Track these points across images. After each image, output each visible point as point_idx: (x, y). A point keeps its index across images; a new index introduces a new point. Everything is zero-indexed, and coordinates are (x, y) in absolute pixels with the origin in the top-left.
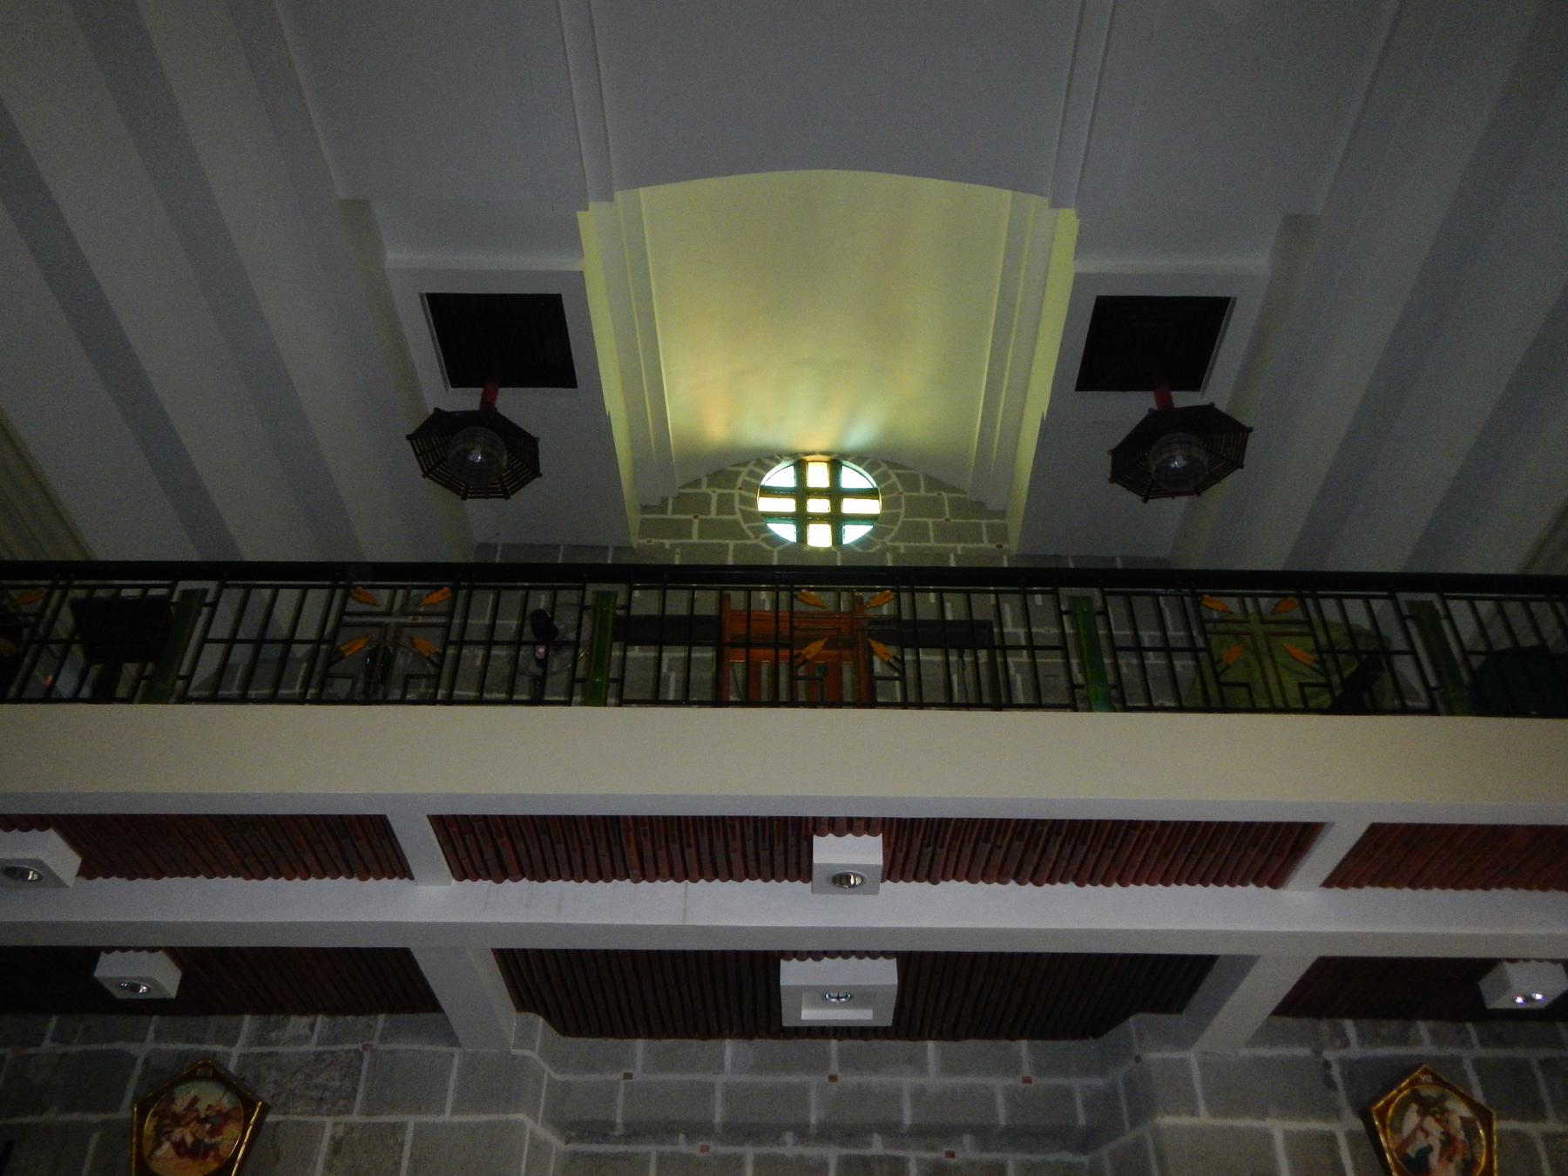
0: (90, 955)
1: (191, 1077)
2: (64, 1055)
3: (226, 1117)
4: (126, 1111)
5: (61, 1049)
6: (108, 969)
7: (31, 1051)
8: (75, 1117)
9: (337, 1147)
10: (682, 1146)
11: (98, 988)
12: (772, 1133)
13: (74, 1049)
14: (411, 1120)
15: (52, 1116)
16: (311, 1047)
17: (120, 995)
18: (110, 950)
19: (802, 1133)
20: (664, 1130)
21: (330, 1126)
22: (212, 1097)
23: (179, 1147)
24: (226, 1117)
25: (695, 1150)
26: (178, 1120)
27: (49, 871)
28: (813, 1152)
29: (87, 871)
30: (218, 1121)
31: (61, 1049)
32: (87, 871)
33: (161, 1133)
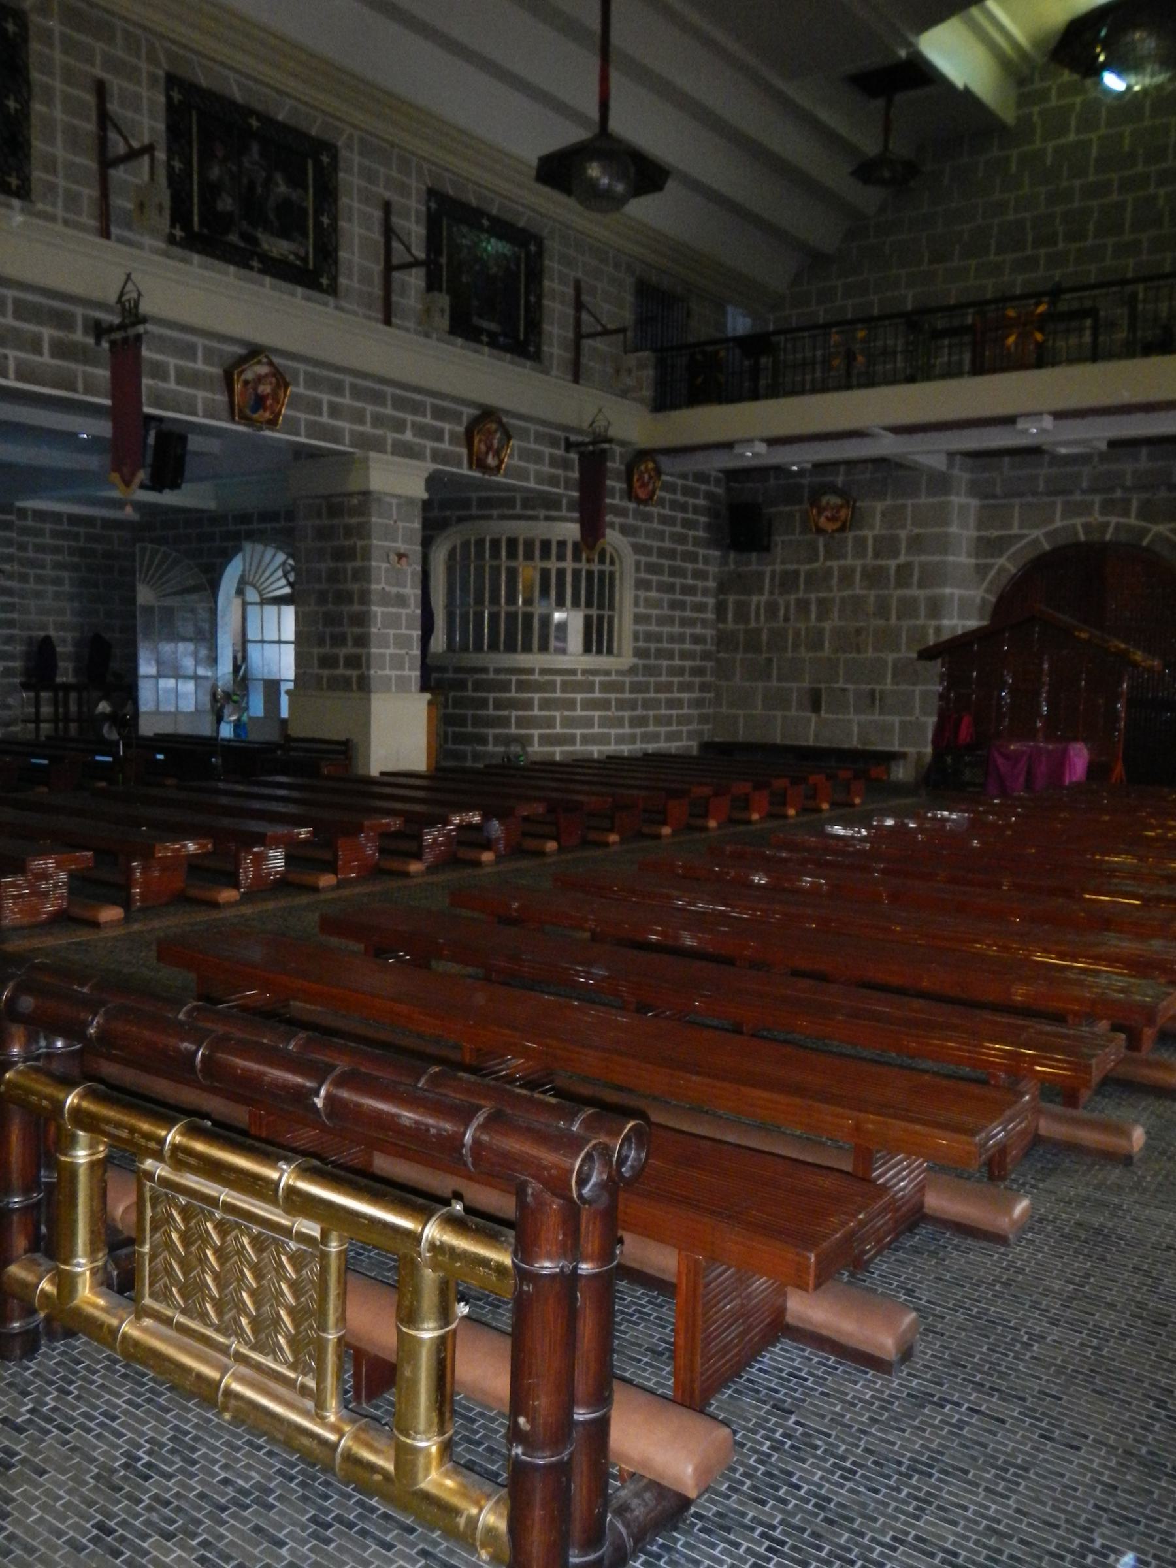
1: (825, 493)
3: (840, 507)
4: (806, 506)
9: (883, 515)
10: (1030, 499)
12: (1071, 492)
14: (910, 502)
16: (868, 476)
19: (1084, 492)
20: (1021, 495)
21: (879, 506)
22: (835, 500)
23: (828, 519)
24: (840, 507)
25: (1035, 500)
26: (825, 509)
28: (1088, 498)
30: (838, 508)
33: (819, 513)
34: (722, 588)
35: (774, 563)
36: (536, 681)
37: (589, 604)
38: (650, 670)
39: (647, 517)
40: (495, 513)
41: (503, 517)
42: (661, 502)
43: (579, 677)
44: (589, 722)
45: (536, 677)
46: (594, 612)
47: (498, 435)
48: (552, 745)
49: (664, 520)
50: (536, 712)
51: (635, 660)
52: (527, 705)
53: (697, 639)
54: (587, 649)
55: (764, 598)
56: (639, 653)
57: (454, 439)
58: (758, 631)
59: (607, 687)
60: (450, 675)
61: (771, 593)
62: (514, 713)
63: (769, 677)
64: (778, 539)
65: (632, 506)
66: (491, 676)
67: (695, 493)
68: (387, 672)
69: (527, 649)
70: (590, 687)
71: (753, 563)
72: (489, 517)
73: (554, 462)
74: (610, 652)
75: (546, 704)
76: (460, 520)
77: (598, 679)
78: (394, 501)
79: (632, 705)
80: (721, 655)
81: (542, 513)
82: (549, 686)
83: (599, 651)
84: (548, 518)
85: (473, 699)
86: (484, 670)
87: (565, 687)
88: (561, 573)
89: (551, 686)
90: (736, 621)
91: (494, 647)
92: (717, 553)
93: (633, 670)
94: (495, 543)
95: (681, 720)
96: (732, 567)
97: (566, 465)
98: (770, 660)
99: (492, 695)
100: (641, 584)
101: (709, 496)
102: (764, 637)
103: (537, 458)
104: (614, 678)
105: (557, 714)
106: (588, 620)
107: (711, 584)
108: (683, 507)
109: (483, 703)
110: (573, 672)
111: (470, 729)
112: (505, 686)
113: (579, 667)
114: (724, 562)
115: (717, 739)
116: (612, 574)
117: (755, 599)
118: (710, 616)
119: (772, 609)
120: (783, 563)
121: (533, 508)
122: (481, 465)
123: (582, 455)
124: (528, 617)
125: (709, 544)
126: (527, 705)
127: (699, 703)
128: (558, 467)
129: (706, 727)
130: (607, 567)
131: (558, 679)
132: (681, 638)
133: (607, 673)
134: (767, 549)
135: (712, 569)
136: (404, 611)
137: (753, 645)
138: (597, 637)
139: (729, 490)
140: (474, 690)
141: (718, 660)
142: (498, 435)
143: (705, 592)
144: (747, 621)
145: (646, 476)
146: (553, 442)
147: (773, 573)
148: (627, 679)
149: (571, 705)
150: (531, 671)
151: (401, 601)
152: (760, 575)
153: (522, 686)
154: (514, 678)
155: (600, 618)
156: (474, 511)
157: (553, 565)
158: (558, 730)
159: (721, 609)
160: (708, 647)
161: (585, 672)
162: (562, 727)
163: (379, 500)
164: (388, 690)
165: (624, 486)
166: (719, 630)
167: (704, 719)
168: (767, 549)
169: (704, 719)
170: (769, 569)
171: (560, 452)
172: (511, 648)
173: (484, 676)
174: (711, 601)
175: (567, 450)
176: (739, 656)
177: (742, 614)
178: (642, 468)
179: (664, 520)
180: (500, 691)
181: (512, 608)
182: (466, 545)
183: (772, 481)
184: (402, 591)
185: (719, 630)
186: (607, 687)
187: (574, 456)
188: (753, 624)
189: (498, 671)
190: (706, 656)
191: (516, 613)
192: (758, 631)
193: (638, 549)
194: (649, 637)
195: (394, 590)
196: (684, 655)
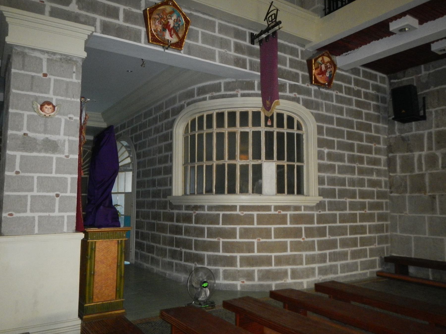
0: (428, 46)
2: (429, 74)
5: (428, 72)
6: (435, 48)
7: (420, 75)
8: (438, 88)
11: (433, 53)
13: (431, 71)
15: (432, 89)
17: (440, 53)
18: (433, 42)
27: (412, 26)
29: (421, 23)
31: (428, 72)
32: (421, 23)
34: (390, 149)
35: (431, 127)
36: (238, 215)
37: (280, 157)
38: (333, 206)
39: (328, 97)
40: (208, 96)
41: (212, 98)
42: (339, 88)
43: (273, 212)
44: (283, 247)
45: (238, 212)
46: (285, 163)
47: (174, 17)
48: (252, 265)
49: (340, 100)
50: (238, 240)
51: (321, 198)
52: (232, 234)
53: (373, 184)
54: (280, 190)
55: (424, 153)
56: (322, 193)
57: (128, 17)
58: (422, 176)
59: (296, 219)
60: (184, 211)
61: (430, 148)
62: (222, 240)
63: (433, 210)
64: (432, 111)
65: (314, 88)
66: (206, 212)
67: (366, 86)
68: (29, 214)
69: (232, 191)
70: (283, 219)
71: (413, 129)
72: (205, 99)
73: (238, 48)
74: (300, 192)
75: (245, 233)
76: (188, 104)
77: (289, 213)
78: (45, 57)
79: (321, 232)
80: (392, 195)
81: (241, 92)
82: (249, 220)
83: (291, 192)
84: (243, 95)
85: (195, 228)
86: (202, 207)
87: (261, 219)
88: (257, 135)
89: (249, 220)
90: (403, 171)
91: (209, 191)
92: (386, 126)
93: (320, 206)
94: (210, 117)
95: (364, 242)
96: (398, 134)
97: (251, 52)
98: (434, 197)
99: (206, 226)
100: (321, 143)
101: (377, 88)
102: (427, 180)
103: (224, 44)
104: (303, 212)
105: (255, 241)
106: (280, 168)
107: (382, 146)
108: (357, 93)
109: (201, 232)
110: (268, 208)
111: (193, 251)
112: (214, 220)
113: (273, 204)
114: (391, 131)
115: (394, 255)
116: (299, 137)
117: (416, 154)
118: (383, 167)
119: (432, 161)
120: (437, 126)
121: (233, 90)
122: (155, 39)
123: (260, 42)
124: (232, 168)
125: (378, 119)
126: (232, 234)
127: (379, 229)
128: (243, 53)
129: (385, 246)
130: (295, 131)
131: (255, 213)
132: (361, 183)
133: (297, 208)
134: (424, 118)
135: (383, 137)
136: (55, 156)
137: (418, 187)
138: (289, 182)
139: (391, 84)
140: (196, 223)
141: (391, 198)
142: (174, 17)
143: (378, 151)
144: (412, 170)
145: (323, 66)
146: (239, 35)
147: (430, 134)
148: (315, 213)
149: (267, 233)
150: (233, 208)
151: (53, 146)
152: (420, 138)
153: (228, 219)
154: (221, 213)
155: (291, 168)
156: (196, 98)
157: (250, 129)
158: (256, 254)
159: (391, 163)
160: (383, 189)
161: (277, 208)
162: (259, 251)
163: (24, 55)
164: (30, 232)
165: (307, 74)
166: (390, 177)
167: (382, 240)
168: (424, 118)
169: (382, 240)
170: (426, 132)
171: (247, 43)
172: (220, 191)
173: (202, 212)
174: (383, 158)
175: (252, 42)
176: (407, 195)
177: (407, 165)
178: (320, 60)
179: (340, 100)
180: (212, 223)
181: (221, 162)
182: (193, 122)
183: (423, 73)
184: (53, 137)
185: (390, 177)
186: (296, 219)
187: (257, 47)
188: (417, 172)
189: (211, 208)
190: (381, 195)
191: (224, 165)
192: (422, 176)
193: (319, 118)
194: (332, 181)
195: (41, 137)
196: (363, 195)
